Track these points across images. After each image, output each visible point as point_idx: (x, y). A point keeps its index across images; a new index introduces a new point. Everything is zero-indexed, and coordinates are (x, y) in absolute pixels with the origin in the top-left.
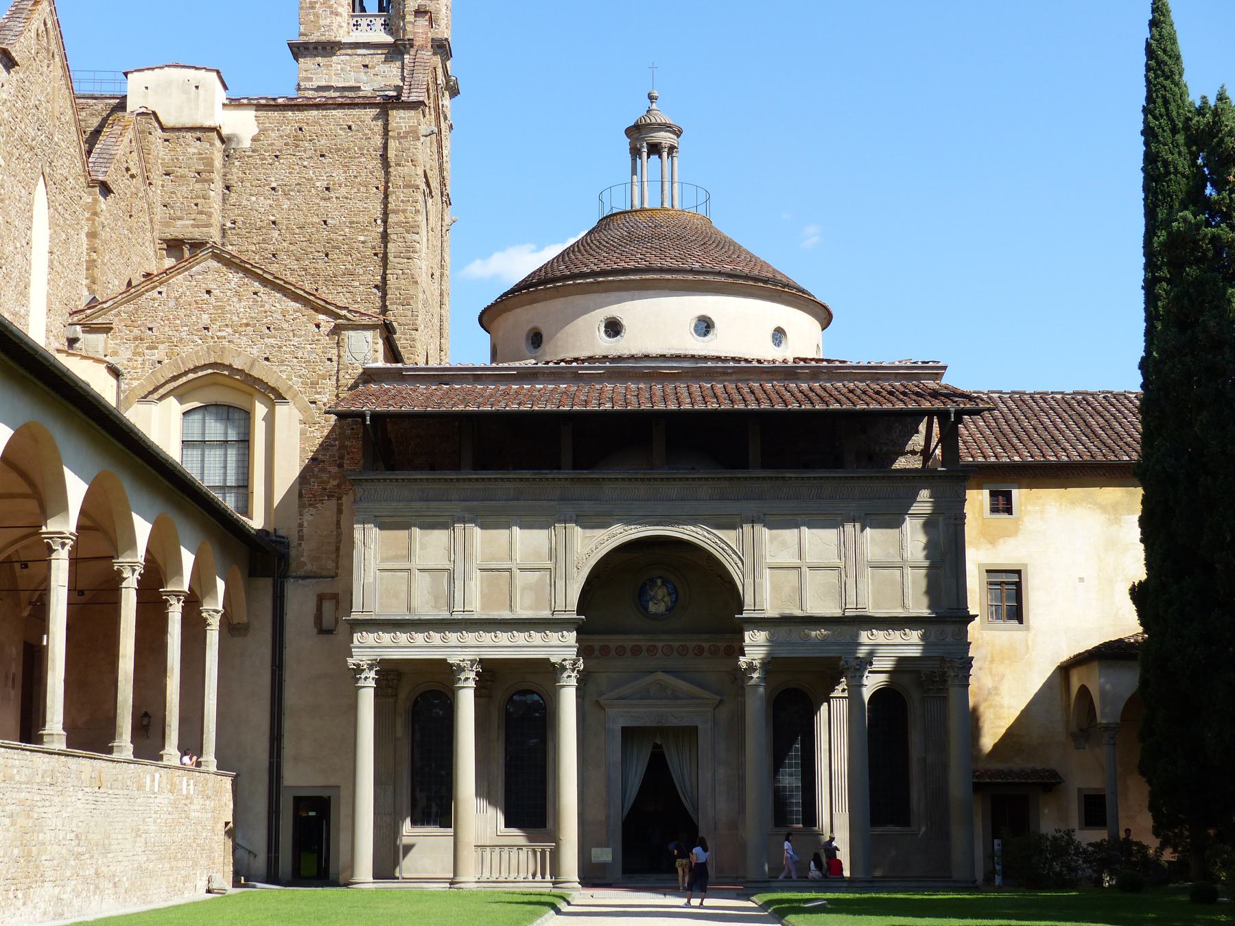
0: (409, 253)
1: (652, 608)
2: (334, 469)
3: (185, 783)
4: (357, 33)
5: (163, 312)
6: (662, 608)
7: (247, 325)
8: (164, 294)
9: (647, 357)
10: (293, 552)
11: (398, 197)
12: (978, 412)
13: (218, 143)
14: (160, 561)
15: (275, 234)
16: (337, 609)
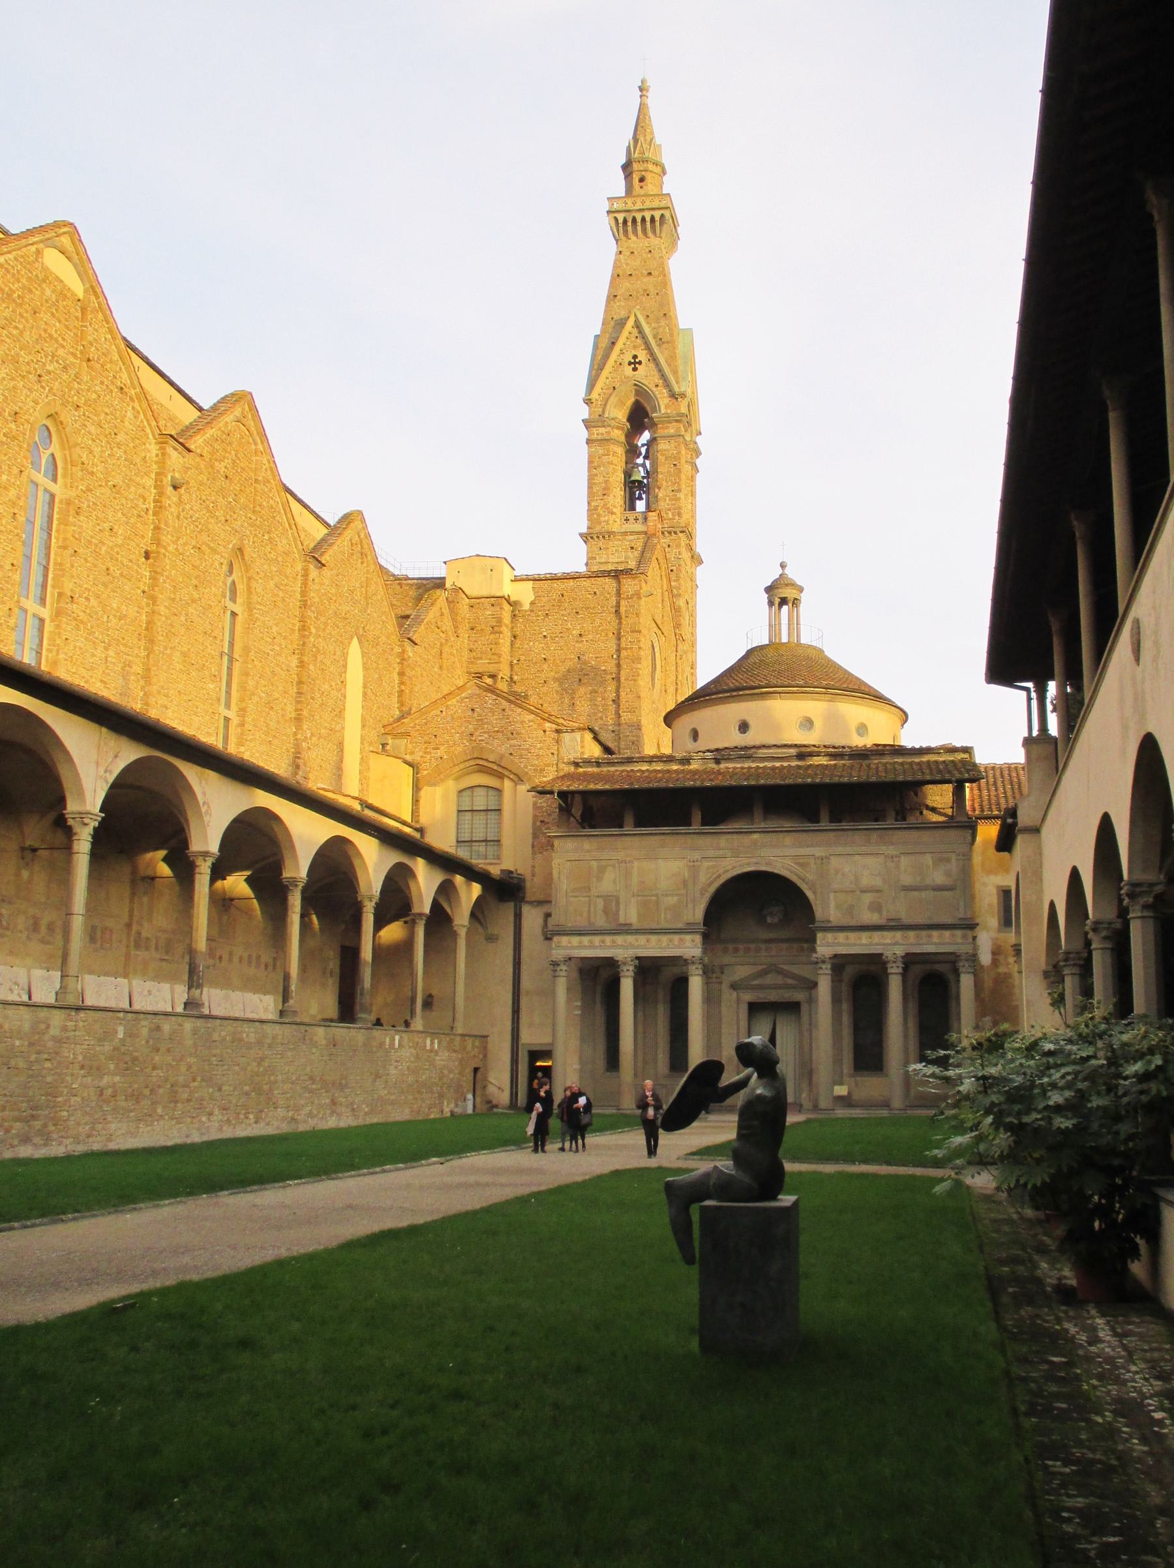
0: (635, 677)
1: (769, 920)
3: (428, 1042)
4: (627, 525)
6: (776, 920)
7: (498, 731)
10: (528, 885)
11: (627, 639)
13: (507, 607)
15: (545, 666)
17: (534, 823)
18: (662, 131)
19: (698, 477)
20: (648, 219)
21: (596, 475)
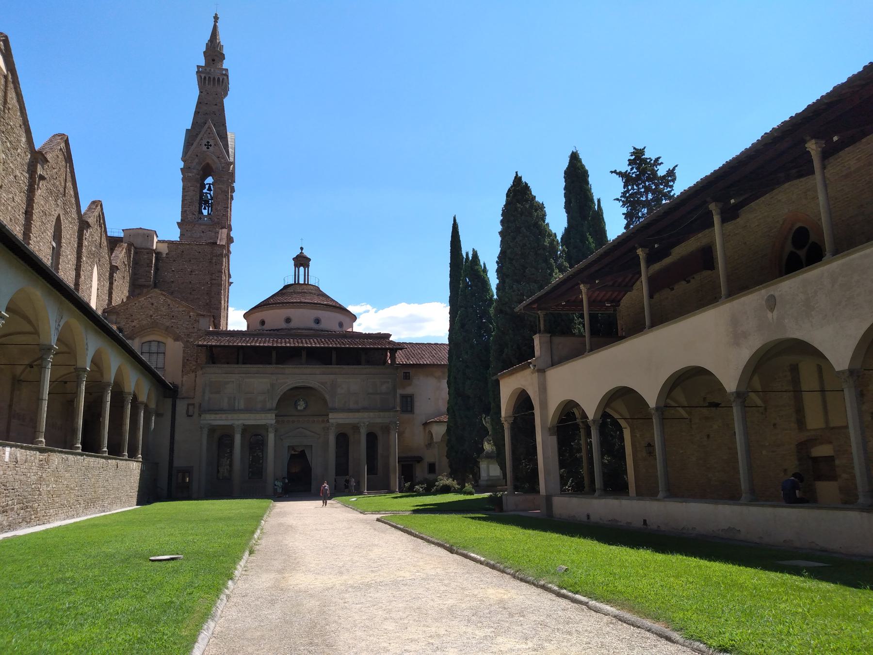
1: (299, 408)
2: (195, 363)
5: (137, 309)
6: (303, 408)
7: (166, 315)
8: (137, 305)
9: (299, 329)
10: (179, 390)
12: (401, 349)
14: (136, 392)
16: (194, 408)
17: (183, 360)
18: (223, 38)
19: (233, 202)
20: (216, 79)
21: (186, 195)
